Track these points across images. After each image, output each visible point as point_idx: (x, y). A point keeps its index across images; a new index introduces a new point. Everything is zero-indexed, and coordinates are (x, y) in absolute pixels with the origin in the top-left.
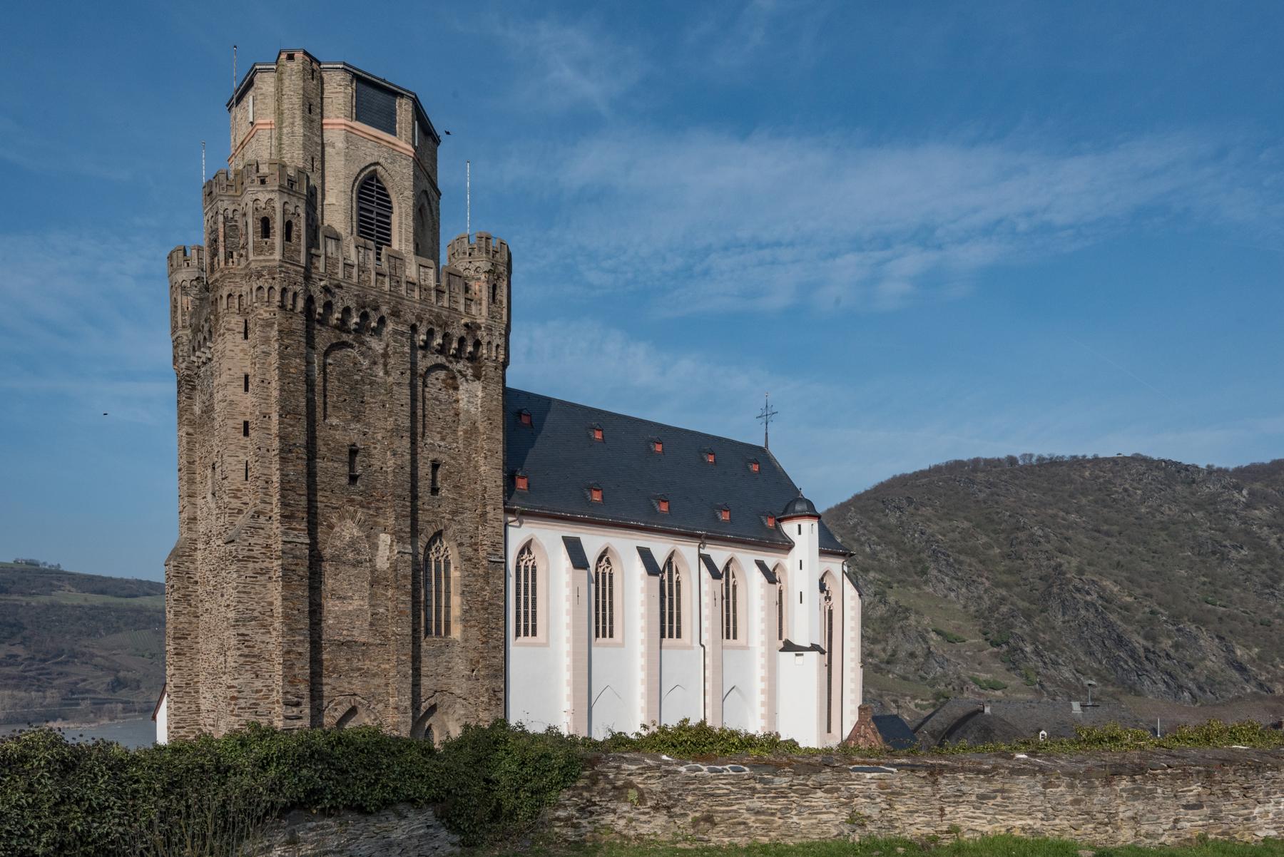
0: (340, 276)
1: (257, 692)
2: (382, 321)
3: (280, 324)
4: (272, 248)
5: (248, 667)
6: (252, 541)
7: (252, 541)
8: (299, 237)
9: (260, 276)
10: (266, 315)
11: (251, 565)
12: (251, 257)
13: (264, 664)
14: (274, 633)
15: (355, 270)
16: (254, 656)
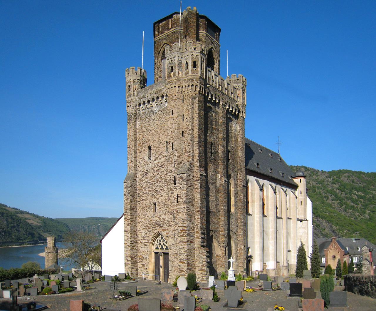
0: (211, 84)
1: (191, 228)
2: (219, 101)
3: (198, 98)
4: (197, 72)
5: (189, 219)
6: (190, 173)
7: (190, 173)
8: (204, 69)
9: (192, 81)
10: (194, 95)
11: (189, 182)
12: (190, 73)
13: (192, 218)
14: (195, 207)
15: (214, 82)
16: (190, 215)
